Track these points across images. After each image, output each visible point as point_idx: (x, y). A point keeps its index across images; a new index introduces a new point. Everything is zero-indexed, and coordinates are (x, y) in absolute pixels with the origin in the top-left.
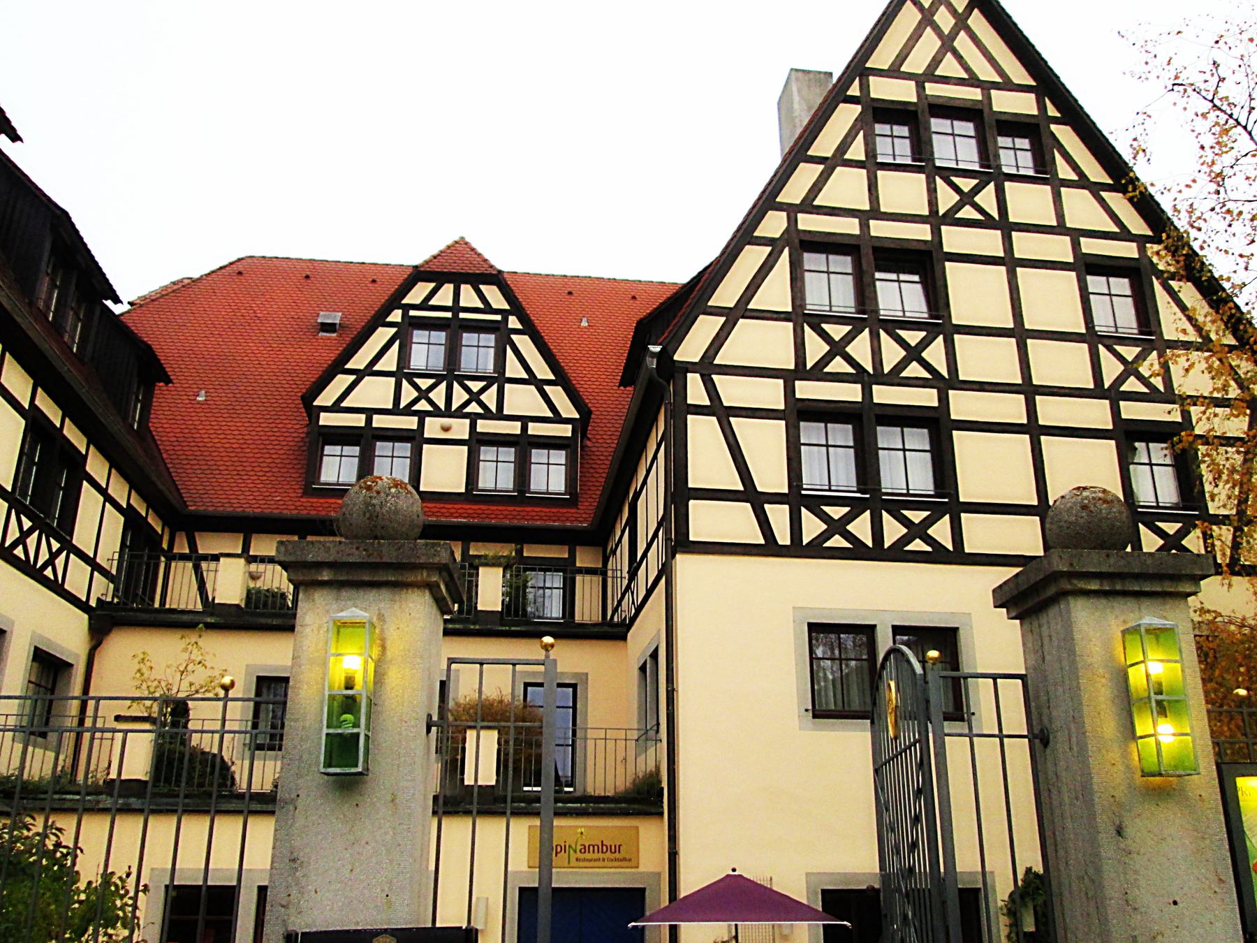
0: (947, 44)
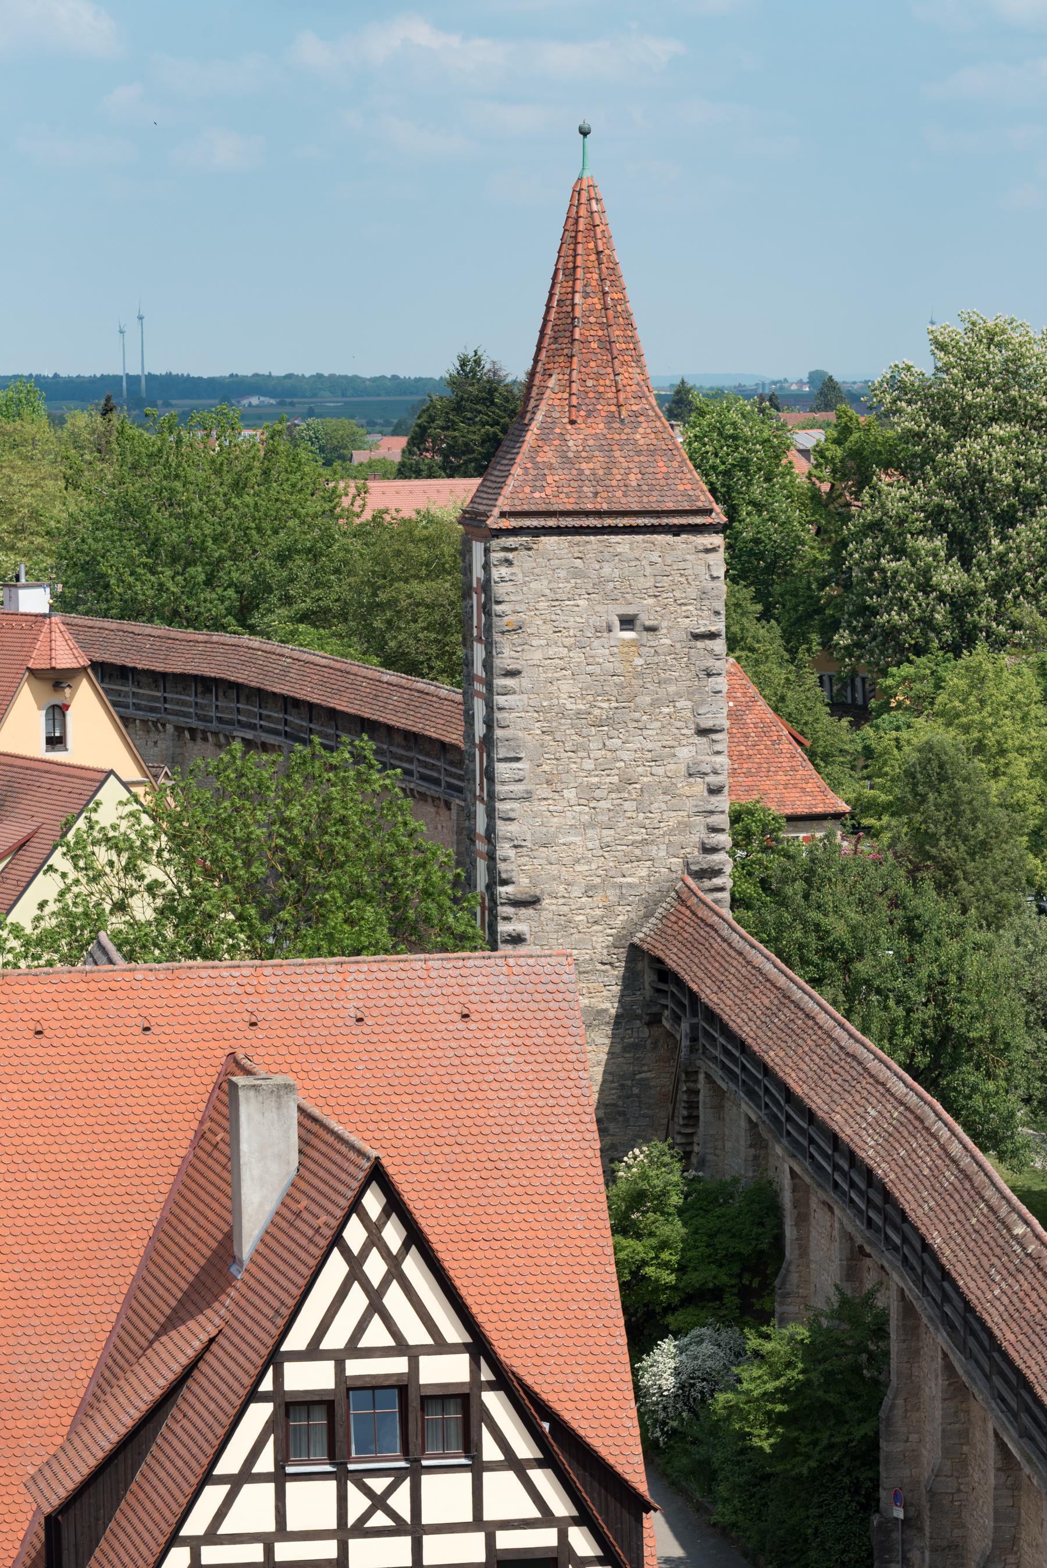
0: (376, 1306)
